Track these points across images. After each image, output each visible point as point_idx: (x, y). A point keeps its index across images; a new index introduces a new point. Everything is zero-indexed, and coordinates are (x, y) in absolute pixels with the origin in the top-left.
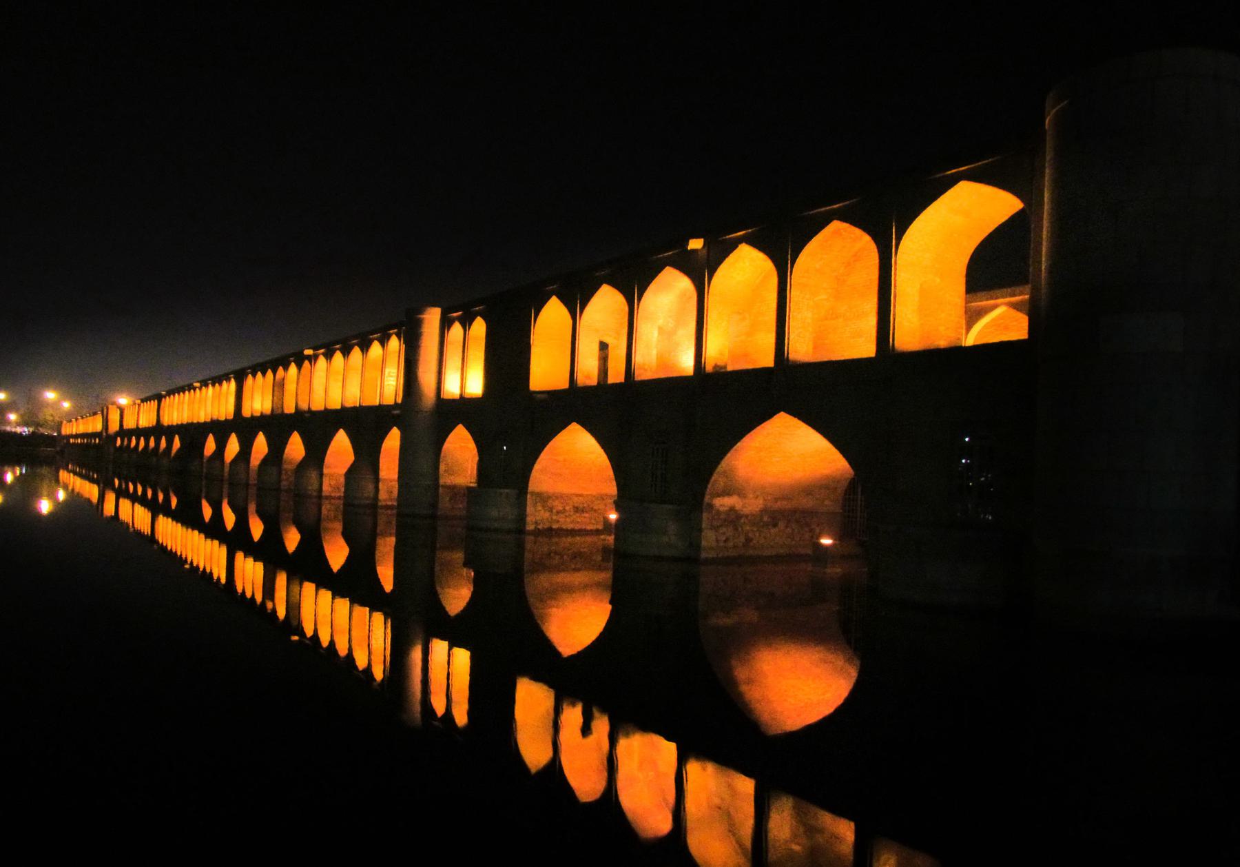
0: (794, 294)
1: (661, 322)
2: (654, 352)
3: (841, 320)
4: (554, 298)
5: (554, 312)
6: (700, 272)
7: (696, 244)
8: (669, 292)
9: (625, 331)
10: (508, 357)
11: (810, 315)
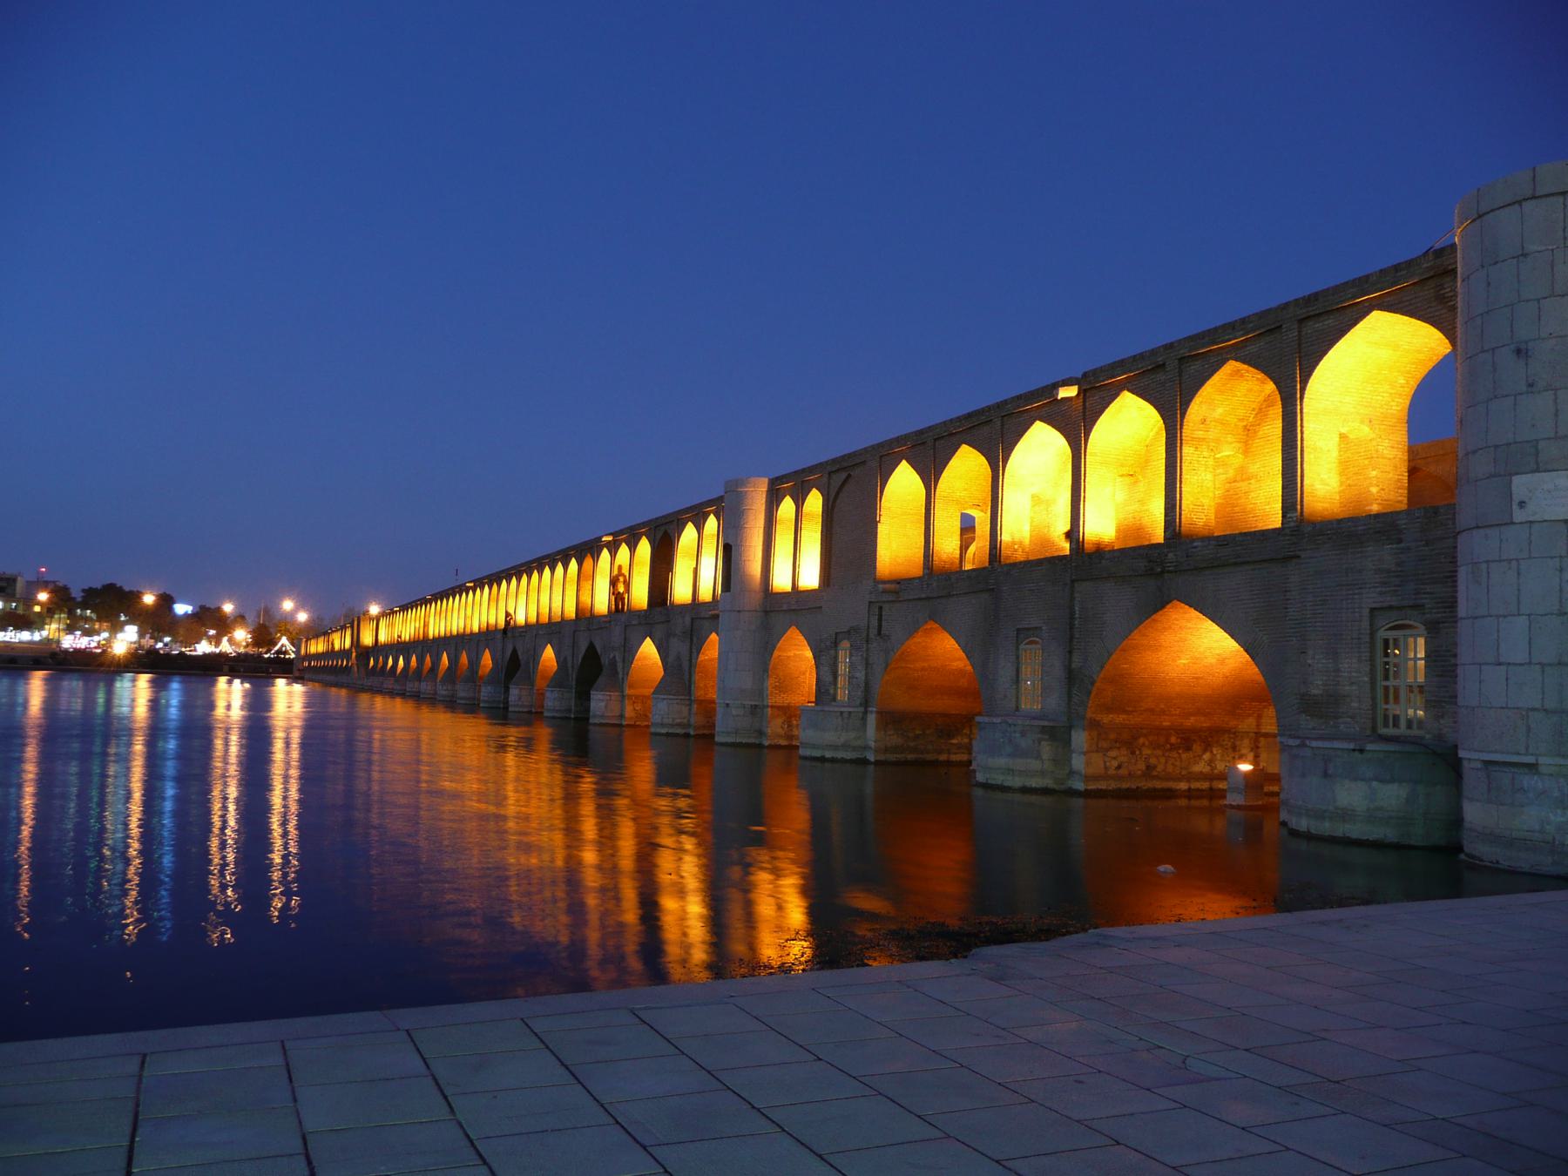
0: (1188, 451)
4: (904, 462)
5: (904, 482)
6: (1076, 427)
11: (1209, 476)
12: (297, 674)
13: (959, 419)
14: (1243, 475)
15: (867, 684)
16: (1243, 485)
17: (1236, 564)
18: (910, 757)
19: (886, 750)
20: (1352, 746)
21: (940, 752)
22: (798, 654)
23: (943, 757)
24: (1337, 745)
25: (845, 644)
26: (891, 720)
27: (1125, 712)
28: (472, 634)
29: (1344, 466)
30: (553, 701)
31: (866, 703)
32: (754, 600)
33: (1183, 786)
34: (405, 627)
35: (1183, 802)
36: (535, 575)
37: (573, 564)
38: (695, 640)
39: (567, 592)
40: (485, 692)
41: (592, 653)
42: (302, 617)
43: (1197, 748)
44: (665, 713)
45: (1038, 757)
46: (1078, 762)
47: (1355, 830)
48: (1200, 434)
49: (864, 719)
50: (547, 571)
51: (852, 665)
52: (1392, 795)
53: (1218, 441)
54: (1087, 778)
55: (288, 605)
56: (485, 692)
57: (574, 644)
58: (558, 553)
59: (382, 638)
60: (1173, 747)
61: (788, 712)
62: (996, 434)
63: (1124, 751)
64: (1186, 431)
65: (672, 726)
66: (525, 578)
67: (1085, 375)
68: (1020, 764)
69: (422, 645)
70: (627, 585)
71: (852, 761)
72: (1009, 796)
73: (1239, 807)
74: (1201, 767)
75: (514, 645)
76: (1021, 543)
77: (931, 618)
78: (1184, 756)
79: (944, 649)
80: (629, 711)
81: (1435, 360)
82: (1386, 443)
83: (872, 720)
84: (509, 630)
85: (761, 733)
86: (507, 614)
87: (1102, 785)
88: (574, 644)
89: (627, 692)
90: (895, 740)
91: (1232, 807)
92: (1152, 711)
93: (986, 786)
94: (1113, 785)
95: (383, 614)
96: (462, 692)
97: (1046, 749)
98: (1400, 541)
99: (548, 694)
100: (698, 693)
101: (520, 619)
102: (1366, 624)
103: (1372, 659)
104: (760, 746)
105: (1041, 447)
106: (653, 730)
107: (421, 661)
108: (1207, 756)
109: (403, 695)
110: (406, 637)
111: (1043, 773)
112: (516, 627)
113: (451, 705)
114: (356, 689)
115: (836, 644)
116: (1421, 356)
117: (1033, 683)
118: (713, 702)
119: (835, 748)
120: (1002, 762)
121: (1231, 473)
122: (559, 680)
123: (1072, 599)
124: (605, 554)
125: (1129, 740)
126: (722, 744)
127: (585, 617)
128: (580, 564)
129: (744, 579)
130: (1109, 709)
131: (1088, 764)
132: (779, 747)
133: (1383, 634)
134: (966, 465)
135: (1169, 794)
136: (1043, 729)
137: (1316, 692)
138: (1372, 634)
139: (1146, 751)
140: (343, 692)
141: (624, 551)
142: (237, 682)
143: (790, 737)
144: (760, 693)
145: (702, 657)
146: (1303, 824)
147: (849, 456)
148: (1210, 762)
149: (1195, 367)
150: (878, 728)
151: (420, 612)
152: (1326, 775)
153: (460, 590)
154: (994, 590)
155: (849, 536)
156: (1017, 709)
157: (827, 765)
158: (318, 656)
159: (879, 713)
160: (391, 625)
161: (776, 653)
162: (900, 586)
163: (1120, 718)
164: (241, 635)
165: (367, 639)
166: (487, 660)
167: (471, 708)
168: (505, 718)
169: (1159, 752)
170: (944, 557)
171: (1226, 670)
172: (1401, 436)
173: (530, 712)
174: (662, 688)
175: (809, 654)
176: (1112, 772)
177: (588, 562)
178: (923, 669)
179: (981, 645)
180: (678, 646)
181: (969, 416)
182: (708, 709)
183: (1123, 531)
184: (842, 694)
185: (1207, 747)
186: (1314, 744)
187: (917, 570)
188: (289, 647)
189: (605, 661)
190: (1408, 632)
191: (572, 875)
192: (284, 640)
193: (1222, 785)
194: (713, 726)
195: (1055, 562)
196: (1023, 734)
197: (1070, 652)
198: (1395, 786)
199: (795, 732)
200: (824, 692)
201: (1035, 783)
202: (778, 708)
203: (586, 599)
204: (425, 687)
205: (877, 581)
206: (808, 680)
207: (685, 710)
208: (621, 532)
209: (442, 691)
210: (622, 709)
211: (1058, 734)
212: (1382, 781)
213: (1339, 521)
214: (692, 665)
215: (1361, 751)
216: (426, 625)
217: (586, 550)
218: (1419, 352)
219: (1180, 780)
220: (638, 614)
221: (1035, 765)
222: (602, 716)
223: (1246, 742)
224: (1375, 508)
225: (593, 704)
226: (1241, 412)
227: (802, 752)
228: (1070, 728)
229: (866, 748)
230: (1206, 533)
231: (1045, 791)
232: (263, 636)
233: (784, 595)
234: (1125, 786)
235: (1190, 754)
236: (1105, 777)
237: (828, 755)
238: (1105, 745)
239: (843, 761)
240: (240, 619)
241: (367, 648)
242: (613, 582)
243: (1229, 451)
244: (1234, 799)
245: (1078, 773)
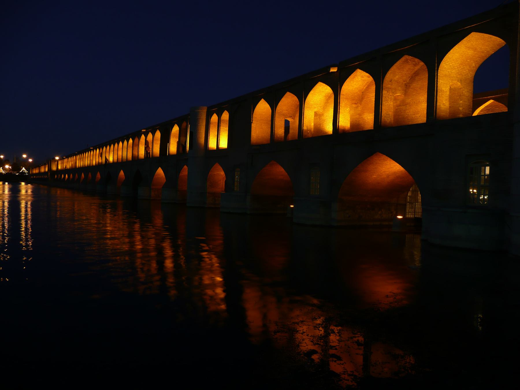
0: (384, 92)
1: (316, 110)
2: (313, 124)
4: (263, 100)
5: (263, 107)
6: (336, 84)
7: (334, 70)
8: (320, 94)
9: (298, 115)
10: (239, 130)
11: (392, 103)
14: (403, 103)
22: (219, 174)
28: (93, 166)
29: (451, 98)
34: (68, 164)
36: (116, 145)
37: (131, 141)
55: (24, 156)
64: (384, 85)
66: (112, 146)
69: (74, 170)
76: (310, 131)
81: (488, 56)
82: (466, 90)
101: (111, 159)
110: (68, 167)
116: (483, 54)
121: (398, 102)
124: (143, 137)
127: (135, 159)
134: (288, 100)
141: (150, 136)
145: (181, 174)
153: (88, 150)
158: (36, 174)
161: (210, 173)
165: (54, 168)
166: (98, 175)
172: (471, 88)
175: (222, 173)
177: (136, 140)
183: (352, 125)
188: (26, 171)
192: (24, 169)
195: (327, 137)
203: (136, 153)
206: (222, 184)
216: (76, 163)
217: (136, 136)
218: (483, 52)
224: (461, 116)
232: (16, 167)
233: (213, 151)
241: (54, 171)
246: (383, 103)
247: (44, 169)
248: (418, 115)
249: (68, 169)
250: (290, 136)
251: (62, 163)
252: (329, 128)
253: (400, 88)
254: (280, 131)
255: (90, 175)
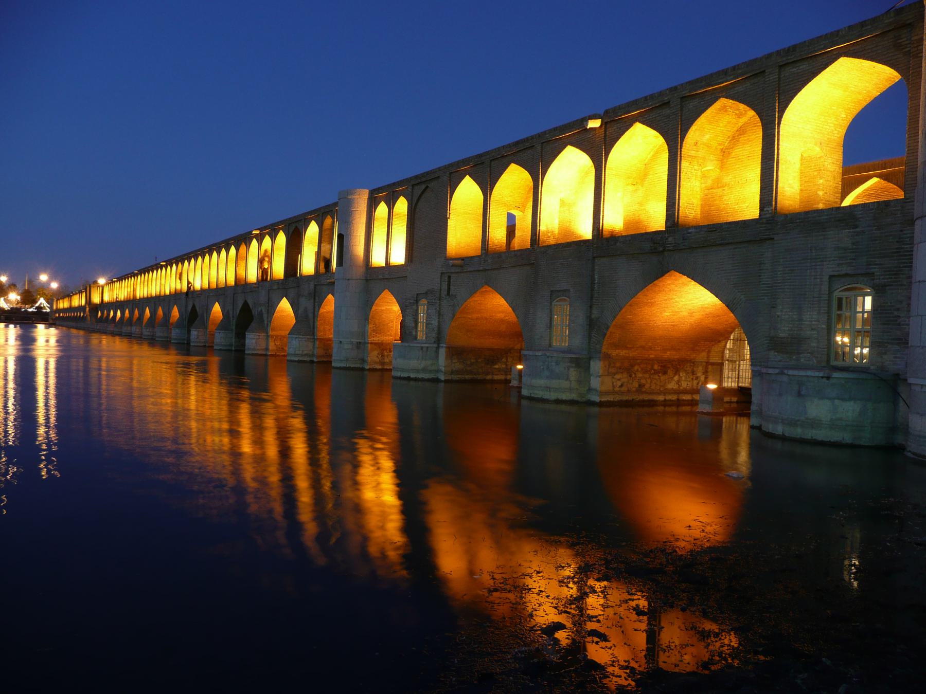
0: (685, 166)
3: (726, 188)
4: (468, 177)
5: (468, 191)
6: (598, 149)
7: (594, 124)
9: (530, 204)
11: (698, 184)
12: (51, 322)
13: (509, 146)
14: (718, 184)
15: (439, 327)
16: (719, 191)
17: (721, 245)
18: (467, 377)
19: (452, 372)
20: (821, 374)
21: (488, 374)
22: (390, 309)
23: (489, 377)
24: (809, 373)
25: (424, 301)
26: (456, 352)
27: (627, 348)
28: (165, 296)
30: (220, 339)
31: (438, 340)
32: (360, 272)
33: (661, 398)
34: (121, 291)
35: (661, 408)
37: (233, 250)
38: (317, 299)
39: (229, 268)
40: (175, 333)
41: (246, 308)
42: (54, 285)
43: (670, 372)
44: (297, 347)
45: (568, 379)
46: (595, 383)
47: (820, 434)
48: (693, 153)
49: (437, 352)
50: (215, 254)
51: (429, 317)
52: (849, 410)
53: (704, 159)
54: (602, 393)
55: (44, 278)
56: (175, 333)
57: (234, 303)
58: (222, 242)
59: (106, 298)
60: (656, 372)
61: (382, 347)
62: (537, 157)
63: (625, 375)
65: (302, 355)
66: (200, 259)
67: (606, 112)
68: (555, 383)
69: (132, 303)
70: (270, 263)
71: (429, 380)
72: (547, 406)
73: (708, 414)
74: (672, 385)
75: (192, 302)
76: (552, 232)
77: (487, 284)
78: (663, 378)
79: (495, 305)
80: (272, 346)
81: (869, 100)
83: (442, 352)
84: (190, 292)
85: (363, 361)
86: (189, 283)
87: (610, 398)
88: (234, 303)
89: (271, 333)
90: (458, 366)
91: (702, 413)
92: (643, 347)
93: (530, 399)
94: (617, 398)
95: (107, 284)
96: (159, 332)
97: (573, 373)
98: (855, 227)
99: (217, 335)
100: (320, 334)
101: (197, 286)
102: (825, 287)
103: (829, 313)
104: (363, 369)
105: (572, 163)
106: (288, 358)
107: (132, 313)
108: (676, 378)
109: (120, 335)
111: (570, 390)
112: (194, 291)
113: (152, 342)
114: (90, 331)
115: (417, 302)
116: (860, 97)
117: (562, 326)
118: (330, 340)
119: (418, 371)
120: (542, 382)
121: (709, 182)
122: (224, 325)
123: (593, 270)
124: (254, 243)
125: (628, 367)
126: (337, 368)
127: (241, 285)
128: (237, 250)
129: (352, 258)
130: (617, 346)
131: (602, 383)
132: (376, 370)
133: (837, 294)
134: (514, 178)
135: (652, 403)
136: (572, 360)
137: (782, 335)
138: (830, 293)
139: (639, 375)
140: (82, 332)
141: (267, 241)
142: (12, 326)
143: (383, 364)
144: (363, 334)
145: (322, 310)
146: (779, 429)
147: (427, 173)
148: (678, 382)
149: (692, 104)
150: (446, 358)
151: (132, 281)
152: (799, 394)
153: (156, 267)
154: (535, 265)
155: (427, 228)
156: (550, 346)
157: (412, 383)
158: (64, 310)
159: (448, 348)
160: (112, 290)
161: (374, 308)
162: (464, 262)
163: (623, 353)
164: (14, 296)
165: (96, 299)
166: (175, 313)
167: (166, 345)
168: (188, 350)
169: (647, 376)
170: (496, 242)
171: (692, 320)
172: (838, 156)
173: (205, 346)
174: (295, 330)
175: (396, 308)
176: (617, 389)
177: (243, 248)
178: (477, 319)
179: (523, 301)
180: (305, 303)
181: (517, 143)
182: (327, 345)
183: (627, 224)
184: (421, 335)
185: (677, 372)
186: (791, 372)
187: (479, 253)
189: (255, 312)
190: (857, 292)
191: (235, 454)
193: (697, 397)
194: (331, 356)
196: (557, 363)
197: (591, 307)
198: (852, 403)
199: (387, 360)
200: (407, 332)
201: (564, 396)
202: (375, 344)
203: (241, 272)
204: (135, 329)
205: (447, 259)
207: (310, 345)
208: (266, 228)
209: (146, 332)
210: (267, 344)
211: (582, 364)
212: (843, 400)
213: (799, 214)
214: (315, 316)
215: (828, 378)
216: (135, 290)
217: (242, 240)
218: (860, 93)
219: (658, 394)
220: (278, 282)
221: (565, 384)
222: (254, 349)
223: (700, 368)
224: (821, 206)
225: (247, 341)
226: (720, 139)
227: (394, 373)
228: (590, 359)
229: (438, 371)
230: (694, 223)
231: (572, 402)
232: (28, 297)
233: (380, 269)
234: (625, 398)
235: (666, 377)
236: (614, 393)
237: (413, 376)
238: (612, 370)
239: (423, 380)
240: (12, 286)
242: (261, 261)
243: (711, 167)
244: (703, 408)
245: (596, 390)
246: (682, 183)
247: (78, 301)
248: (745, 205)
249: (121, 301)
250: (517, 243)
251: (112, 290)
252: (586, 232)
253: (712, 157)
254: (498, 234)
255: (160, 312)
